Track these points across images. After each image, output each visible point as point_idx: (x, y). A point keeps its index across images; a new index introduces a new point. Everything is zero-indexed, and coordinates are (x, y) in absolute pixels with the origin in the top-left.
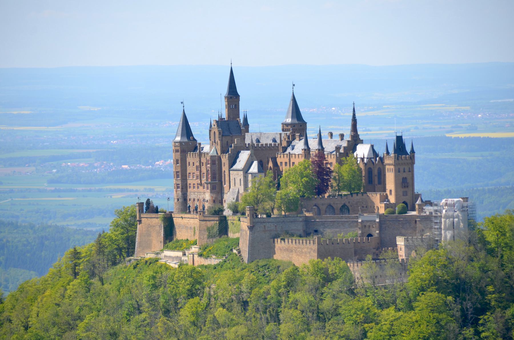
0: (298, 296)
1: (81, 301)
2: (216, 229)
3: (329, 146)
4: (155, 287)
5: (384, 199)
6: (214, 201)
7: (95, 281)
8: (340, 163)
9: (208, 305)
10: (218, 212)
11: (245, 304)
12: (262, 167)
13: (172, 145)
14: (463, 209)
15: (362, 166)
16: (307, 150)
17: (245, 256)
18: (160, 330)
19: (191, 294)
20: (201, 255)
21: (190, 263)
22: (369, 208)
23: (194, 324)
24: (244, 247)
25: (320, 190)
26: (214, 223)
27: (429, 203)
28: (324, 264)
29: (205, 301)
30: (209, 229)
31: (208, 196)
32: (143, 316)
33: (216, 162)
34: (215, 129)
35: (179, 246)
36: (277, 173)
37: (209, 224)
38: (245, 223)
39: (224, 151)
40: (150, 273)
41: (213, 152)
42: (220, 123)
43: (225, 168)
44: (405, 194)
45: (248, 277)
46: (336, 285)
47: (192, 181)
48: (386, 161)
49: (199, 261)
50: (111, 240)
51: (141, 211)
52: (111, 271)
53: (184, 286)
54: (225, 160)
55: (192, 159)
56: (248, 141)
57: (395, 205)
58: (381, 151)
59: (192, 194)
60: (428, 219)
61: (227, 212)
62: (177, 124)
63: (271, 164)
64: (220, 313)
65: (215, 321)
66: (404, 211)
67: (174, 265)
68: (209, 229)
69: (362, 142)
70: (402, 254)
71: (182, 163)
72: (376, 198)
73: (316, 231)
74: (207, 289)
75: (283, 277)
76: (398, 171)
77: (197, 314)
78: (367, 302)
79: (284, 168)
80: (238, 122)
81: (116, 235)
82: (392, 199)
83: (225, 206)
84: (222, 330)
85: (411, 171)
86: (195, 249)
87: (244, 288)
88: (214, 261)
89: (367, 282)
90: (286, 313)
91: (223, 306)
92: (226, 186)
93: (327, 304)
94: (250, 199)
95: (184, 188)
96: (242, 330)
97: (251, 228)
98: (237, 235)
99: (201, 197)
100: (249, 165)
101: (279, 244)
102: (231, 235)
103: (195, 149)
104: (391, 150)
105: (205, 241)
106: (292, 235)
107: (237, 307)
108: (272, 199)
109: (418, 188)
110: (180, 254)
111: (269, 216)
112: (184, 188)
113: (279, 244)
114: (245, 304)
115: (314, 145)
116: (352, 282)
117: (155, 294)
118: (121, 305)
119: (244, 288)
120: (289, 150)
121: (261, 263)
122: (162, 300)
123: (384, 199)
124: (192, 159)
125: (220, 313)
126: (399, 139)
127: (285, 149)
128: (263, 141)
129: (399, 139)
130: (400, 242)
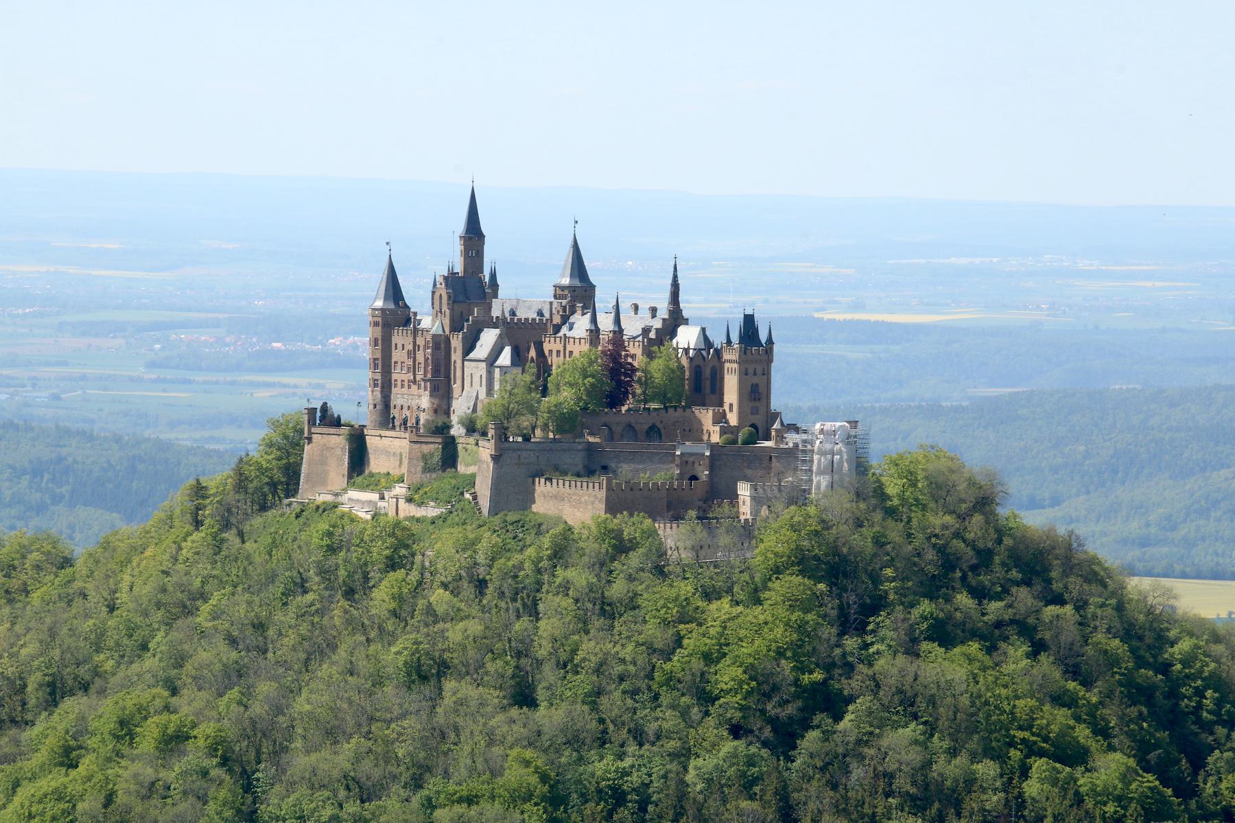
0: (571, 574)
1: (204, 568)
2: (437, 458)
3: (632, 327)
4: (332, 550)
5: (720, 418)
6: (436, 411)
7: (231, 536)
8: (650, 355)
9: (420, 583)
10: (442, 430)
11: (481, 585)
12: (519, 358)
14: (850, 440)
15: (685, 362)
16: (595, 332)
17: (485, 504)
18: (337, 621)
19: (392, 565)
20: (410, 500)
21: (392, 513)
22: (693, 432)
23: (394, 614)
24: (484, 489)
25: (615, 398)
26: (434, 448)
27: (794, 428)
28: (616, 522)
29: (414, 576)
30: (424, 457)
31: (425, 401)
32: (310, 597)
33: (441, 345)
34: (442, 291)
36: (544, 368)
37: (426, 449)
38: (486, 450)
39: (455, 328)
40: (324, 526)
41: (436, 329)
42: (451, 279)
43: (456, 356)
44: (755, 411)
45: (488, 540)
46: (634, 559)
47: (398, 375)
48: (726, 356)
49: (407, 510)
50: (260, 468)
51: (312, 422)
52: (257, 521)
53: (380, 551)
54: (457, 342)
55: (401, 338)
56: (496, 312)
57: (738, 428)
58: (718, 340)
59: (399, 397)
60: (792, 453)
61: (457, 430)
63: (533, 353)
64: (439, 598)
65: (430, 610)
66: (751, 440)
68: (424, 457)
69: (686, 322)
70: (746, 509)
71: (384, 344)
72: (706, 416)
73: (605, 468)
74: (418, 558)
75: (546, 541)
76: (744, 374)
77: (399, 598)
78: (685, 588)
79: (555, 361)
80: (481, 281)
82: (733, 419)
83: (454, 419)
84: (441, 625)
85: (767, 373)
87: (481, 558)
88: (431, 511)
89: (687, 556)
90: (550, 602)
91: (445, 586)
92: (456, 387)
93: (618, 589)
94: (497, 411)
95: (386, 386)
96: (475, 627)
97: (496, 458)
98: (472, 470)
99: (414, 403)
101: (542, 487)
102: (461, 468)
104: (735, 338)
105: (418, 477)
107: (468, 590)
108: (533, 412)
109: (777, 402)
110: (375, 497)
111: (527, 439)
113: (542, 487)
114: (481, 585)
115: (606, 323)
116: (662, 554)
117: (332, 561)
118: (272, 578)
119: (481, 558)
121: (511, 517)
122: (342, 573)
123: (720, 418)
124: (401, 338)
125: (439, 598)
126: (749, 320)
127: (557, 329)
128: (522, 314)
129: (749, 320)
130: (744, 490)
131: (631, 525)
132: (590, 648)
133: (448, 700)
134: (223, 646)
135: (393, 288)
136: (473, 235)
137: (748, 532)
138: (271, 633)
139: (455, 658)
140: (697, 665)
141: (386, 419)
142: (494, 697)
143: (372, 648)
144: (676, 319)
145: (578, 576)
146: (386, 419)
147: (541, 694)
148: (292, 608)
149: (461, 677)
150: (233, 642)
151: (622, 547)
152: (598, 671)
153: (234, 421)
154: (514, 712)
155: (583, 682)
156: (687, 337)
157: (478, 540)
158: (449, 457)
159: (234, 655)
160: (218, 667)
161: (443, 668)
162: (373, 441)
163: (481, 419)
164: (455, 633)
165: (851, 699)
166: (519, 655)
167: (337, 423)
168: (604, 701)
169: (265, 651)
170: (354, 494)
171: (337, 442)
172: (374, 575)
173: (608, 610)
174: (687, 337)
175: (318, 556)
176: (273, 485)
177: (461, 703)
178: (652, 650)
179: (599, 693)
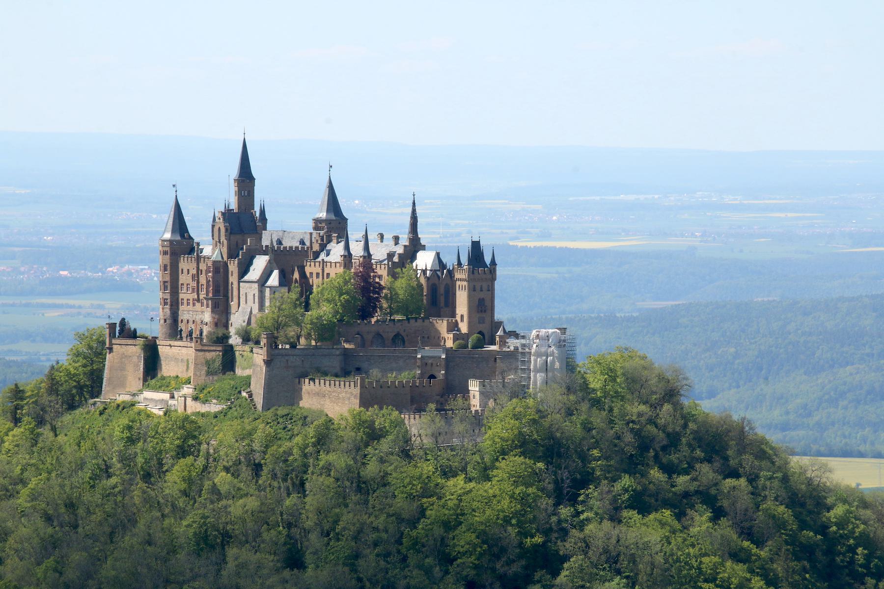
0: (332, 457)
1: (23, 457)
2: (218, 363)
3: (379, 252)
4: (131, 441)
5: (453, 327)
6: (216, 325)
7: (46, 432)
8: (393, 275)
9: (205, 468)
10: (222, 340)
11: (257, 468)
12: (285, 280)
13: (157, 245)
14: (561, 344)
15: (423, 281)
16: (348, 257)
17: (259, 400)
18: (137, 500)
19: (182, 452)
20: (196, 399)
21: (180, 410)
22: (434, 340)
23: (185, 493)
24: (258, 388)
25: (365, 312)
26: (215, 355)
27: (516, 335)
28: (370, 413)
29: (201, 462)
30: (208, 363)
31: (207, 316)
32: (113, 480)
33: (220, 270)
34: (221, 224)
35: (165, 385)
36: (306, 287)
37: (209, 356)
38: (259, 356)
39: (232, 255)
40: (125, 421)
41: (216, 256)
42: (228, 215)
43: (233, 279)
44: (481, 321)
45: (262, 431)
46: (385, 445)
47: (185, 295)
48: (457, 276)
49: (193, 407)
50: (69, 374)
51: (112, 335)
52: (67, 418)
53: (171, 441)
54: (233, 267)
55: (186, 265)
56: (265, 242)
57: (467, 336)
58: (450, 261)
59: (185, 313)
60: (512, 355)
61: (235, 340)
62: (168, 218)
63: (296, 275)
64: (222, 479)
65: (215, 490)
66: (479, 344)
67: (157, 411)
68: (208, 363)
69: (423, 248)
70: (475, 403)
71: (172, 270)
72: (442, 326)
73: (358, 369)
74: (204, 447)
75: (311, 431)
76: (472, 290)
77: (189, 481)
78: (427, 468)
79: (315, 282)
80: (252, 216)
81: (76, 367)
82: (464, 328)
83: (232, 330)
84: (224, 502)
85: (491, 289)
86: (187, 390)
87: (256, 446)
88: (214, 407)
89: (427, 442)
90: (315, 482)
91: (227, 469)
92: (233, 304)
93: (372, 469)
94: (269, 323)
95: (174, 304)
96: (252, 503)
97: (268, 363)
98: (247, 372)
99: (198, 318)
100: (266, 275)
101: (307, 386)
102: (239, 372)
103: (191, 250)
104: (464, 260)
105: (202, 379)
106: (325, 374)
107: (246, 472)
108: (298, 324)
109: (500, 314)
110: (166, 396)
111: (293, 346)
112: (174, 304)
113: (307, 386)
114: (257, 468)
115: (357, 250)
116: (407, 440)
117: (131, 450)
118: (81, 466)
119: (256, 446)
120: (322, 256)
121: (282, 411)
122: (140, 460)
123: (453, 327)
124: (186, 265)
125: (222, 479)
126: (476, 246)
127: (317, 255)
128: (287, 243)
129: (476, 246)
130: (474, 387)
131: (383, 417)
132: (348, 519)
133: (231, 565)
134: (40, 523)
135: (179, 223)
137: (478, 421)
138: (81, 511)
139: (237, 529)
140: (438, 531)
141: (174, 331)
142: (269, 560)
143: (167, 522)
144: (415, 246)
145: (338, 459)
146: (174, 331)
147: (309, 558)
148: (98, 490)
149: (242, 544)
150: (48, 519)
151: (374, 435)
152: (356, 538)
153: (50, 336)
154: (287, 573)
155: (344, 547)
156: (424, 260)
157: (255, 430)
158: (229, 362)
159: (50, 530)
160: (36, 541)
161: (227, 538)
163: (255, 332)
164: (236, 508)
165: (566, 558)
166: (289, 525)
167: (133, 335)
168: (361, 562)
169: (76, 527)
170: (148, 394)
171: (134, 351)
172: (168, 461)
173: (362, 486)
174: (424, 260)
175: (119, 446)
176: (80, 388)
177: (242, 566)
178: (400, 520)
179: (357, 556)
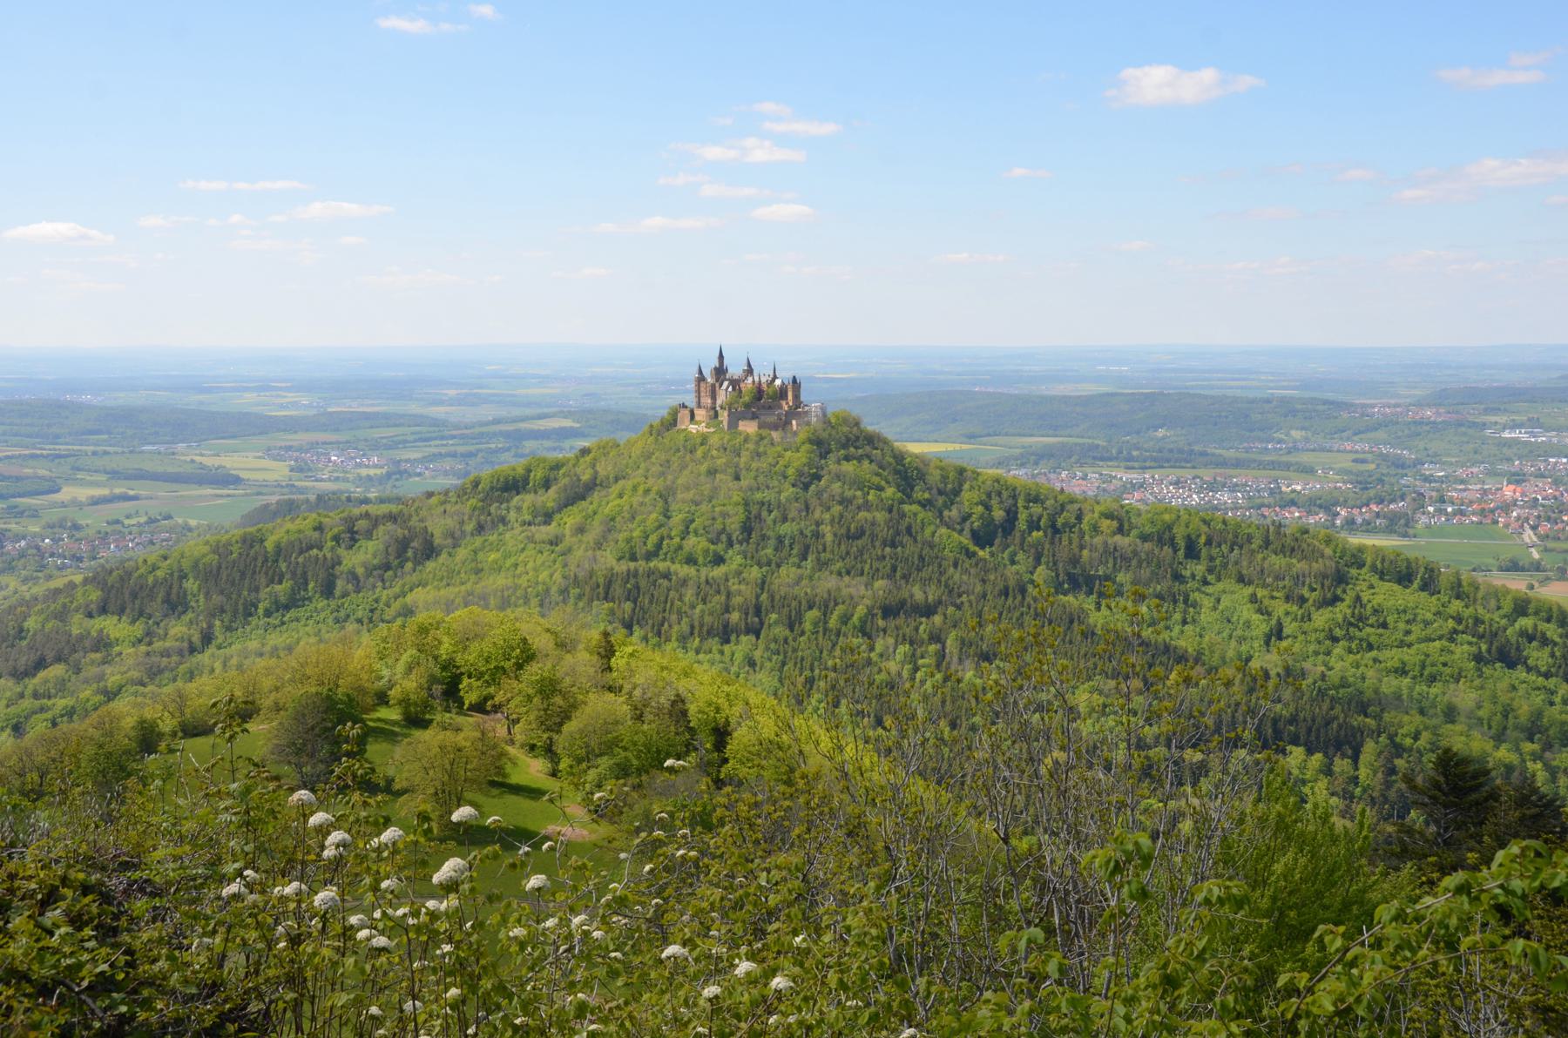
3: (764, 380)
10: (714, 408)
12: (734, 389)
14: (822, 409)
19: (702, 444)
22: (781, 407)
24: (725, 424)
25: (760, 399)
26: (712, 413)
33: (713, 386)
35: (696, 423)
42: (715, 369)
45: (727, 437)
46: (765, 441)
53: (699, 441)
55: (702, 384)
59: (702, 400)
62: (696, 369)
64: (714, 453)
70: (795, 428)
71: (698, 386)
72: (784, 403)
78: (779, 449)
88: (712, 430)
90: (744, 453)
95: (699, 397)
96: (724, 460)
101: (741, 423)
112: (699, 397)
113: (741, 423)
115: (757, 379)
125: (714, 453)
130: (794, 422)
131: (764, 432)
132: (754, 465)
135: (700, 372)
136: (721, 357)
137: (795, 434)
141: (699, 406)
142: (729, 478)
144: (775, 377)
145: (751, 446)
146: (699, 406)
151: (762, 438)
155: (752, 474)
156: (778, 382)
158: (716, 415)
162: (697, 412)
164: (719, 462)
171: (687, 412)
173: (759, 455)
174: (778, 382)
